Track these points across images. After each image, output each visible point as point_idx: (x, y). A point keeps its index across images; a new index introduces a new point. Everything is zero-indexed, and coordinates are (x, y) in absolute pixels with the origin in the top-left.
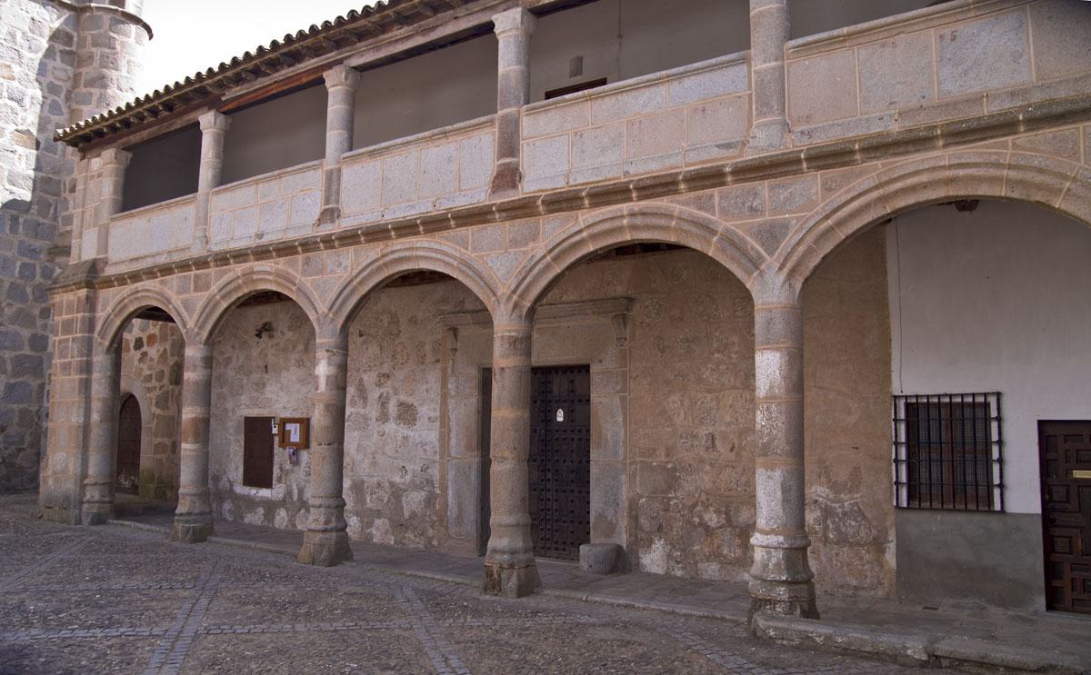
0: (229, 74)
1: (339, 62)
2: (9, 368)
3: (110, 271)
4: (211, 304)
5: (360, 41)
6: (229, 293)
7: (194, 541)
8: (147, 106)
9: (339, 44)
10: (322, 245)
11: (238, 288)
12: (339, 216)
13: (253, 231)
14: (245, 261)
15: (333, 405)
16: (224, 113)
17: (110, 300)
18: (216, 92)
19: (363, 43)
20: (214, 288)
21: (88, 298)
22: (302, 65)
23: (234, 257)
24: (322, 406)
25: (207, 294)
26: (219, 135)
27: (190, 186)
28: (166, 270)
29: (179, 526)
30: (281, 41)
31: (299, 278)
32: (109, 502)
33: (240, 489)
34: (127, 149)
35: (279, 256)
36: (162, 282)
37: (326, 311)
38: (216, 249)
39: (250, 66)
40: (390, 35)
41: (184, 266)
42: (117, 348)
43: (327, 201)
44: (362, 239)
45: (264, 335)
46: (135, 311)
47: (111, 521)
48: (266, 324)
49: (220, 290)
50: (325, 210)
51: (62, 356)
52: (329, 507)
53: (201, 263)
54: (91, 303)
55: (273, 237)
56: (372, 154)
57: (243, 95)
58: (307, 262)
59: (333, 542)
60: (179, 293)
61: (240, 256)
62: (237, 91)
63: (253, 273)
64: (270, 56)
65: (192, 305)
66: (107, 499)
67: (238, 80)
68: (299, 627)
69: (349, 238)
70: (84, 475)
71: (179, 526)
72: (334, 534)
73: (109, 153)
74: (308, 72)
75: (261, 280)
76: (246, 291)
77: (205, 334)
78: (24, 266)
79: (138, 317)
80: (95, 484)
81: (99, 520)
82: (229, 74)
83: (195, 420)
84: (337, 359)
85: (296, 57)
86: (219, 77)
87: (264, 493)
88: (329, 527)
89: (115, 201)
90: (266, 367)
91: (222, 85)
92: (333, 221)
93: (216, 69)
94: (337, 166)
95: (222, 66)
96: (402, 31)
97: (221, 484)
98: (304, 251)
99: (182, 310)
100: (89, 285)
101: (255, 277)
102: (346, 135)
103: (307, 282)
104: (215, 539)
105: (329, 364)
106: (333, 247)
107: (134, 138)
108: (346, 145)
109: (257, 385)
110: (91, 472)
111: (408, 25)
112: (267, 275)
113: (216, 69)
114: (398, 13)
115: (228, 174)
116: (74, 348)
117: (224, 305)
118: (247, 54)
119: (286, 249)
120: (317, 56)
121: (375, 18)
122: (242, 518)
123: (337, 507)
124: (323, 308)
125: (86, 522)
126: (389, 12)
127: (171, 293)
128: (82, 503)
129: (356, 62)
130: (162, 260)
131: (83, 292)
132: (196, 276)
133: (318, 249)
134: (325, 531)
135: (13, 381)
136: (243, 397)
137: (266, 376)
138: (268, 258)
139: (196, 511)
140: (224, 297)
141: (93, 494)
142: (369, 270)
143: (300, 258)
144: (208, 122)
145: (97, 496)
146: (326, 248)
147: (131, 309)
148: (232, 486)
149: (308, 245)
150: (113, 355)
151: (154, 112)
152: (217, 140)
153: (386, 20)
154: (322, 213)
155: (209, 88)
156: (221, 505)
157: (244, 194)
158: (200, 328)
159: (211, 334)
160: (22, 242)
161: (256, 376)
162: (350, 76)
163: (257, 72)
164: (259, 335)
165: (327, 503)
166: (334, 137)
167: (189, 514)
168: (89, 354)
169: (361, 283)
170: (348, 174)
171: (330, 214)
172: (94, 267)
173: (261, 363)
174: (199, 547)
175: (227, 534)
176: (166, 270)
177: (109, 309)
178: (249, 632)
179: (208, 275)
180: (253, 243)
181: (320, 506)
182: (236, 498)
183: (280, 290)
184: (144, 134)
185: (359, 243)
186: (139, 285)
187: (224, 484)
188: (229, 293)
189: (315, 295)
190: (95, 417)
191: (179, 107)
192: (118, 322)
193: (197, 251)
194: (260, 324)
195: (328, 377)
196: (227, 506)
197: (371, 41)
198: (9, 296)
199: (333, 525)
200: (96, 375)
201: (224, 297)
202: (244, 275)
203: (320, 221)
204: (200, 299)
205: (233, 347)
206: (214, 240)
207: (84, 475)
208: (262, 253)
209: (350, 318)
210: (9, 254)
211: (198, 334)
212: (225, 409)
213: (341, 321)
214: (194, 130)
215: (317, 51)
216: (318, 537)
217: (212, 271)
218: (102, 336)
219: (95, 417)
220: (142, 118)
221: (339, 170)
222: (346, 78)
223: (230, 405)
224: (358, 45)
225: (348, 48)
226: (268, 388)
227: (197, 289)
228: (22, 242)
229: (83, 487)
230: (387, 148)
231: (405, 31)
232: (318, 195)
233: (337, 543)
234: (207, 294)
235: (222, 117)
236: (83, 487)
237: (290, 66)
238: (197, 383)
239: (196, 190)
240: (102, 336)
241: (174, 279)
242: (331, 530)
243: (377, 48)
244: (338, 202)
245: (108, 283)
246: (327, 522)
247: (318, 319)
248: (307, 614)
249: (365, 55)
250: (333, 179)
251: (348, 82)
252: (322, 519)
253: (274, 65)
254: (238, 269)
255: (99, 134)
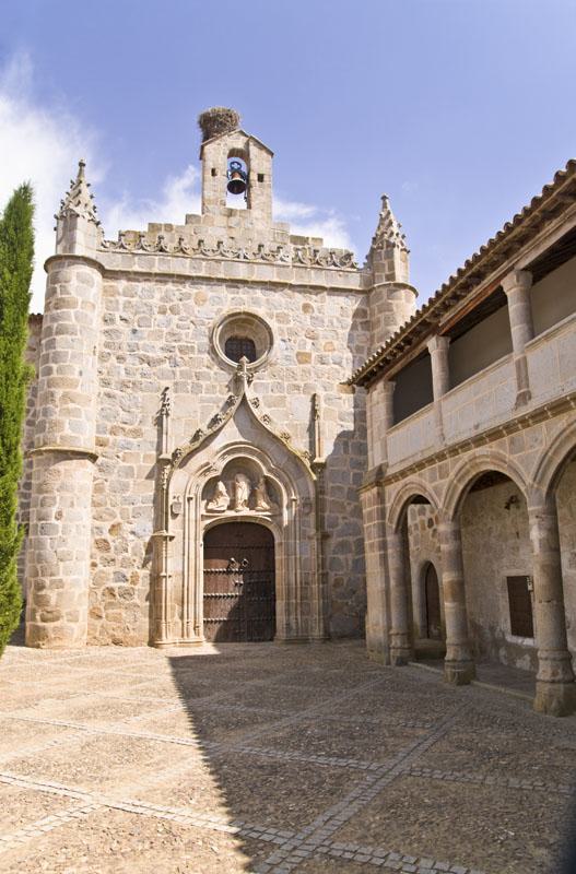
0: (437, 305)
1: (511, 269)
2: (353, 548)
3: (390, 472)
4: (451, 488)
5: (522, 246)
6: (463, 477)
7: (460, 683)
8: (394, 345)
9: (507, 254)
10: (520, 426)
11: (468, 472)
12: (530, 398)
13: (472, 424)
14: (469, 449)
15: (547, 566)
16: (443, 335)
17: (392, 490)
18: (434, 321)
19: (526, 246)
20: (452, 474)
21: (378, 493)
22: (486, 281)
23: (462, 447)
24: (538, 568)
25: (447, 480)
26: (442, 353)
27: (431, 399)
28: (420, 465)
29: (448, 670)
30: (463, 267)
31: (509, 457)
32: (409, 648)
33: (510, 638)
34: (391, 379)
35: (491, 441)
36: (420, 475)
37: (531, 482)
38: (450, 443)
39: (449, 294)
40: (544, 232)
41: (431, 461)
42: (403, 528)
43: (520, 387)
44: (549, 413)
45: (512, 506)
46: (408, 499)
47: (410, 663)
48: (512, 498)
49: (456, 475)
50: (520, 395)
51: (370, 538)
52: (554, 659)
53: (441, 456)
54: (381, 498)
55: (485, 427)
56: (547, 337)
57: (453, 317)
58: (512, 442)
59: (561, 693)
60: (431, 482)
61: (465, 446)
62: (447, 316)
63: (475, 458)
64: (461, 281)
65: (442, 486)
66: (406, 646)
67: (446, 307)
68: (490, 780)
69: (539, 415)
70: (390, 628)
71: (448, 670)
72: (562, 686)
73: (380, 385)
74: (491, 285)
75: (481, 463)
76: (474, 473)
77: (451, 513)
78: (355, 475)
79: (413, 503)
80: (398, 634)
81: (402, 662)
82: (437, 305)
83: (451, 583)
84: (546, 524)
85: (479, 276)
86: (432, 309)
87: (528, 642)
88: (558, 678)
89: (388, 419)
90: (518, 534)
91: (436, 315)
92: (526, 404)
93: (427, 305)
94: (522, 356)
95: (431, 301)
96: (552, 225)
97: (496, 634)
98: (508, 433)
99: (433, 493)
100: (378, 483)
101: (478, 461)
102: (526, 328)
103: (513, 458)
104: (476, 683)
105: (540, 528)
106: (529, 426)
107: (393, 371)
108: (527, 336)
109: (513, 548)
110: (393, 624)
111: (556, 217)
112: (486, 458)
113: (427, 305)
114: (543, 211)
115: (454, 379)
116: (374, 531)
117: (461, 487)
118: (444, 286)
119: (494, 434)
120: (494, 270)
121: (527, 222)
122: (515, 663)
123: (562, 660)
124: (529, 480)
125: (393, 662)
126: (536, 213)
127: (423, 482)
128: (390, 648)
129: (524, 263)
130: (419, 458)
131: (375, 490)
132: (440, 467)
133: (518, 430)
134: (553, 682)
135: (357, 557)
136: (504, 560)
137: (518, 541)
138: (484, 444)
139: (459, 659)
140: (459, 481)
141: (396, 642)
142: (559, 440)
143: (506, 439)
144: (434, 346)
145: (399, 644)
146: (524, 427)
147: (405, 498)
148: (504, 636)
149: (510, 428)
150: (400, 535)
151: (400, 348)
152: (441, 359)
153: (537, 221)
154: (518, 398)
155: (428, 320)
156: (497, 652)
157: (467, 391)
158: (447, 508)
159: (456, 511)
160: (352, 459)
161: (511, 542)
162: (521, 278)
163: (456, 297)
164: (508, 507)
165: (552, 656)
166: (517, 330)
167: (454, 660)
168: (384, 535)
169: (555, 453)
170: (531, 357)
171: (524, 398)
172: (380, 471)
173: (514, 531)
174: (460, 689)
175: (496, 680)
176: (420, 465)
177: (392, 500)
178: (442, 779)
179: (446, 465)
180: (473, 433)
181: (546, 659)
182: (509, 646)
183: (497, 469)
184: (398, 367)
185: (547, 418)
186: (407, 480)
187: (498, 634)
188: (463, 477)
189: (522, 469)
190: (393, 583)
191: (415, 340)
192: (399, 509)
193: (438, 448)
194: (509, 497)
195: (540, 540)
196: (502, 652)
197: (530, 243)
198: (348, 498)
199: (560, 677)
200: (390, 551)
201: (459, 481)
202: (470, 461)
203: (517, 405)
204: (445, 483)
205: (492, 519)
206: (447, 437)
207: (390, 628)
208: (479, 441)
209: (552, 486)
210: (345, 468)
211: (446, 513)
212: (493, 571)
213: (545, 489)
214: (426, 354)
215: (493, 266)
216: (546, 689)
217: (449, 461)
218: (391, 520)
219: (393, 583)
220: (395, 355)
221: (525, 358)
222: (518, 281)
223: (495, 567)
224: (522, 249)
225: (516, 255)
226: (521, 551)
227: (441, 478)
228: (352, 459)
229: (389, 636)
230: (562, 326)
231: (555, 223)
232: (512, 381)
233: (565, 694)
234: (447, 480)
235: (442, 339)
236: (389, 636)
237: (478, 284)
238: (450, 553)
239: (432, 400)
240: (391, 520)
241: (426, 471)
242: (559, 682)
243: (537, 247)
244: (528, 386)
245: (389, 481)
246: (554, 674)
247: (526, 490)
248: (505, 768)
249: (529, 255)
250: (522, 366)
251: (521, 283)
252: (550, 671)
253: (467, 287)
254: (465, 456)
255: (372, 373)
